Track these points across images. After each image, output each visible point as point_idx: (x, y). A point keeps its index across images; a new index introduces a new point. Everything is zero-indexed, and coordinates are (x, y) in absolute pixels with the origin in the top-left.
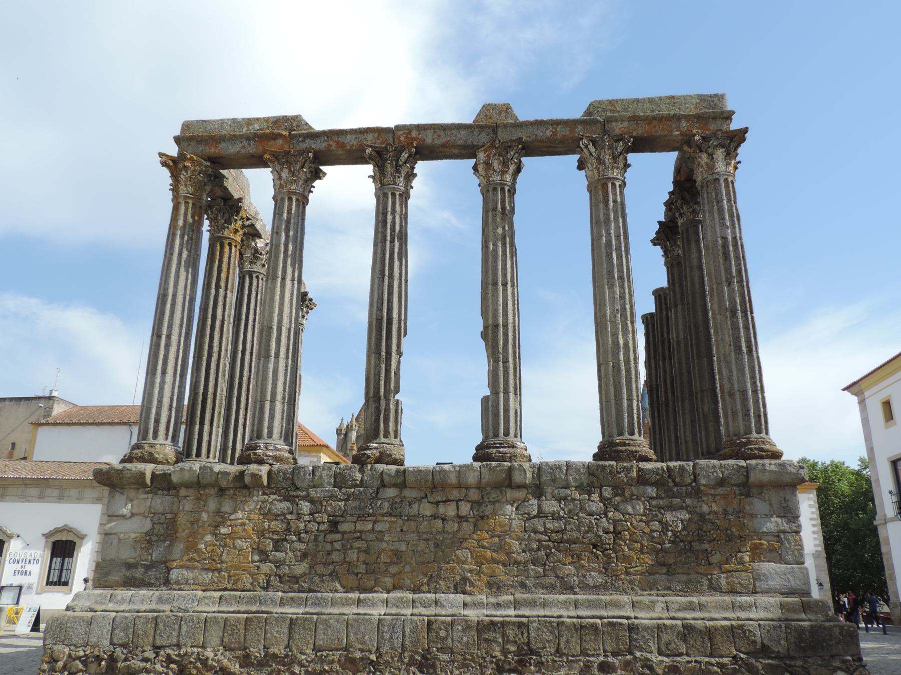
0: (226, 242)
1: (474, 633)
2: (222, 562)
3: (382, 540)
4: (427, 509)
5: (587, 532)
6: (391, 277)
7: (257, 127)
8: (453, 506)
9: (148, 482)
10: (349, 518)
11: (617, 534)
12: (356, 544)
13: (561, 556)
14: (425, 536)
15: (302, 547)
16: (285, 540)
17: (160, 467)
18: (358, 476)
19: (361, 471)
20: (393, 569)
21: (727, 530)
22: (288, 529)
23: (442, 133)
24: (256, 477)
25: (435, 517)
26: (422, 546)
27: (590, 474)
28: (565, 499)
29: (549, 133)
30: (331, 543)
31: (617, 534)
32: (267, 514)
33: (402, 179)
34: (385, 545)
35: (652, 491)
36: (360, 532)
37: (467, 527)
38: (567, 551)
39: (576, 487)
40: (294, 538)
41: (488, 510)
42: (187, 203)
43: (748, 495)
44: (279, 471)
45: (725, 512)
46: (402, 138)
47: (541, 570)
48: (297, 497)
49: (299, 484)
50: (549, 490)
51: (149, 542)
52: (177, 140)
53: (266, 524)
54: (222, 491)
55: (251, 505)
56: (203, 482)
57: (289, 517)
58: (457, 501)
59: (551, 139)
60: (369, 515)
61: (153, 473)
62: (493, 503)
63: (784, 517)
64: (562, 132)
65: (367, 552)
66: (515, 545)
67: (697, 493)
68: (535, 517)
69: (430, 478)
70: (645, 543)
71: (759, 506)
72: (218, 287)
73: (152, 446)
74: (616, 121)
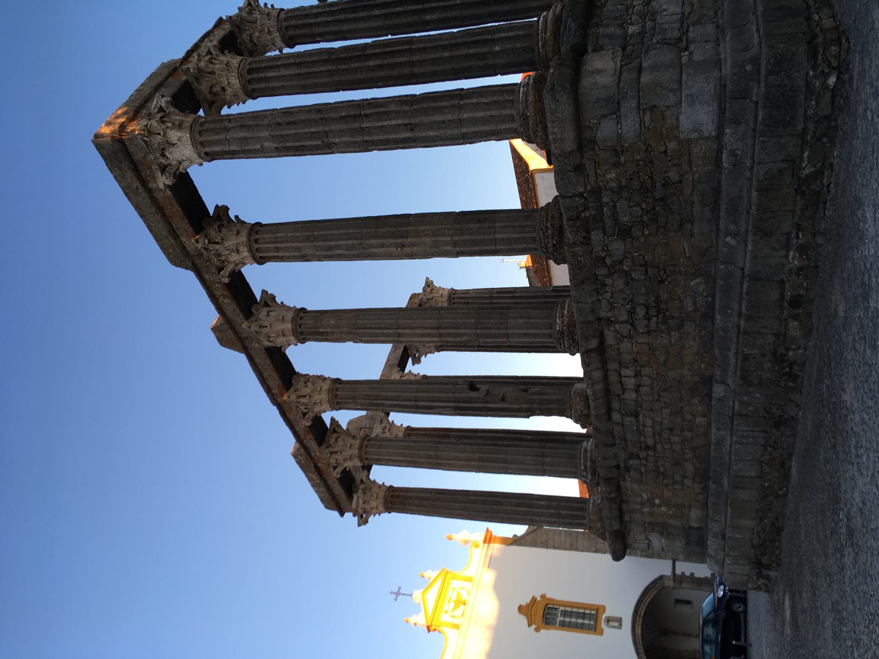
1: (751, 389)
3: (661, 422)
14: (656, 397)
21: (638, 165)
23: (266, 375)
25: (637, 391)
27: (583, 282)
28: (611, 304)
29: (226, 300)
34: (666, 421)
35: (596, 236)
36: (654, 434)
37: (645, 371)
39: (598, 294)
41: (627, 358)
43: (594, 141)
45: (617, 165)
49: (614, 463)
50: (604, 314)
52: (342, 514)
60: (638, 427)
62: (620, 354)
63: (618, 103)
65: (671, 430)
67: (597, 192)
68: (633, 325)
69: (601, 400)
71: (606, 130)
74: (184, 247)
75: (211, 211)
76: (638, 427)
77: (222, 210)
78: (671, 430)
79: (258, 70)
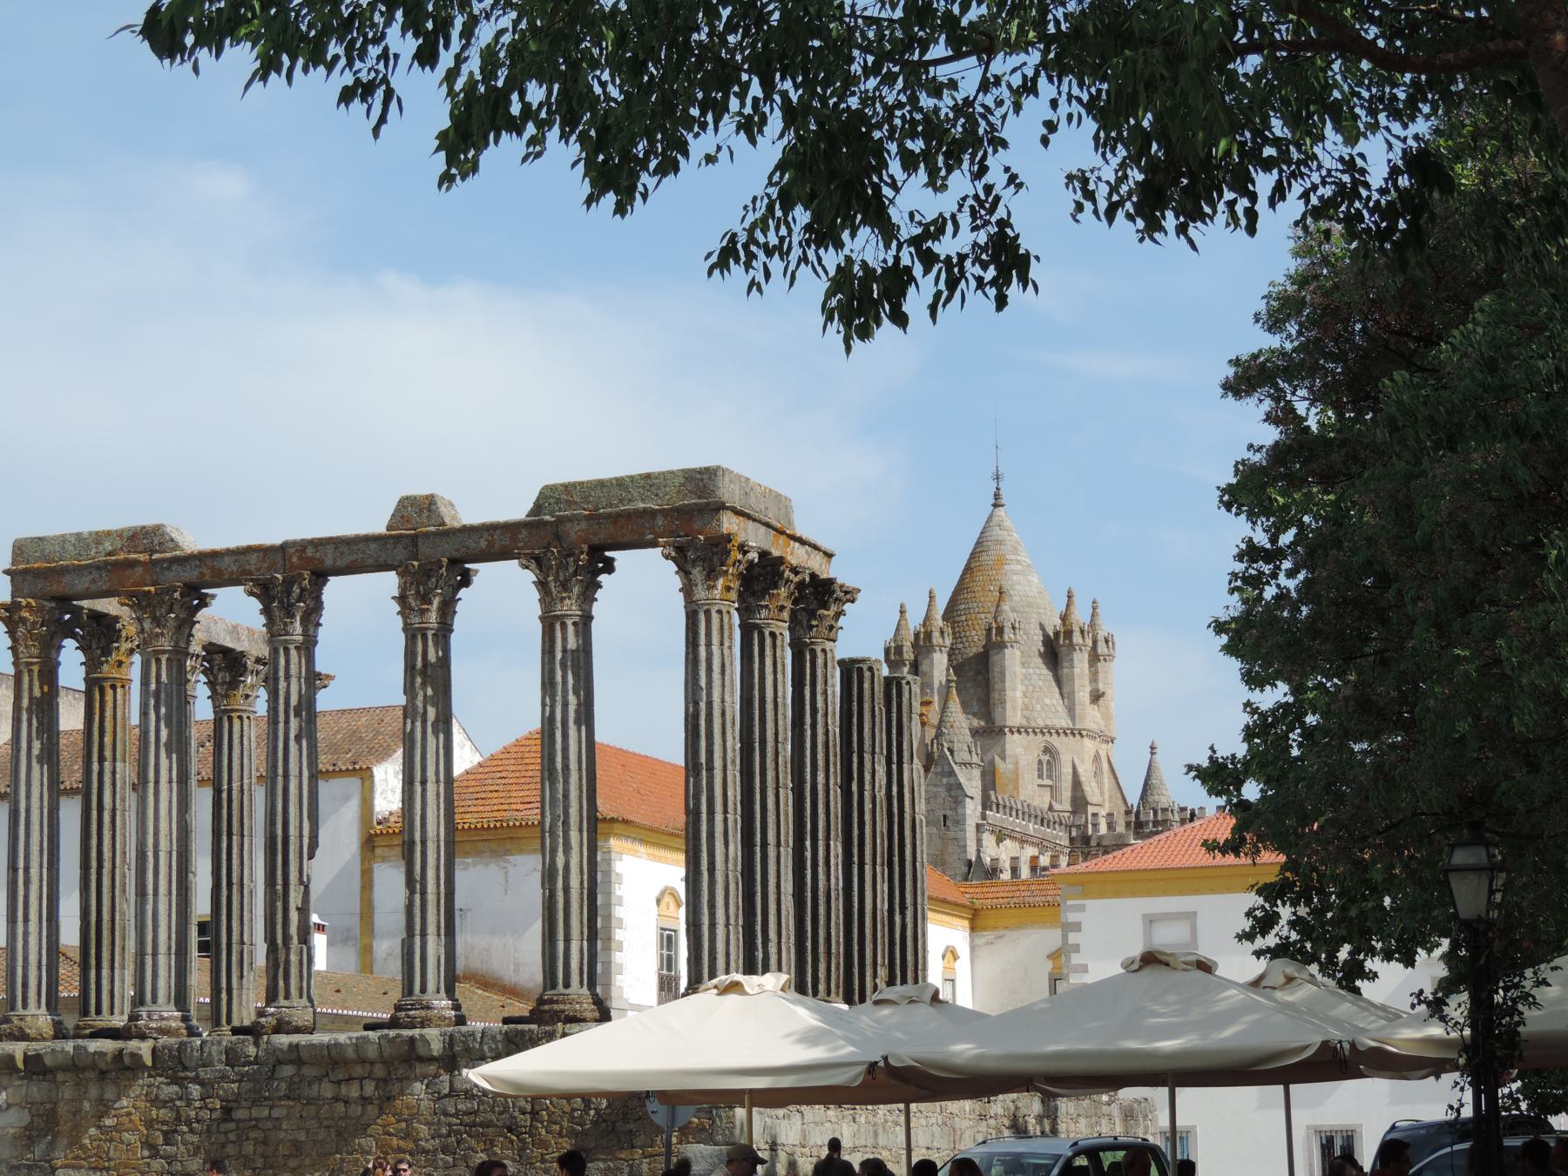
0: (107, 685)
2: (110, 1160)
4: (328, 1091)
5: (501, 1113)
6: (286, 776)
7: (108, 547)
8: (355, 1086)
9: (20, 1065)
10: (244, 1103)
11: (534, 1114)
12: (252, 1135)
13: (473, 1142)
15: (195, 1138)
16: (175, 1131)
17: (34, 1045)
18: (252, 1050)
19: (257, 1044)
20: (293, 1163)
22: (178, 1119)
23: (344, 548)
24: (136, 1057)
25: (336, 1099)
26: (322, 1134)
29: (483, 544)
30: (225, 1133)
31: (534, 1114)
32: (155, 1102)
33: (297, 624)
34: (282, 1135)
37: (372, 1110)
38: (477, 1136)
40: (185, 1129)
42: (30, 671)
44: (164, 1047)
46: (295, 559)
47: (450, 1159)
48: (186, 1078)
49: (187, 1064)
51: (29, 1138)
52: (7, 572)
53: (154, 1112)
54: (103, 1074)
55: (136, 1090)
56: (80, 1064)
57: (178, 1103)
58: (362, 1079)
59: (498, 541)
60: (266, 1099)
61: (26, 1058)
62: (401, 1080)
64: (501, 540)
65: (265, 1143)
66: (424, 1130)
68: (446, 1096)
69: (325, 1052)
70: (565, 1124)
72: (101, 759)
73: (22, 1018)
75: (608, 554)
76: (266, 1099)
77: (609, 567)
78: (265, 1143)
79: (774, 647)
